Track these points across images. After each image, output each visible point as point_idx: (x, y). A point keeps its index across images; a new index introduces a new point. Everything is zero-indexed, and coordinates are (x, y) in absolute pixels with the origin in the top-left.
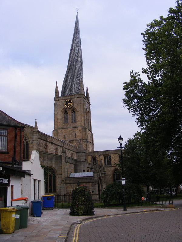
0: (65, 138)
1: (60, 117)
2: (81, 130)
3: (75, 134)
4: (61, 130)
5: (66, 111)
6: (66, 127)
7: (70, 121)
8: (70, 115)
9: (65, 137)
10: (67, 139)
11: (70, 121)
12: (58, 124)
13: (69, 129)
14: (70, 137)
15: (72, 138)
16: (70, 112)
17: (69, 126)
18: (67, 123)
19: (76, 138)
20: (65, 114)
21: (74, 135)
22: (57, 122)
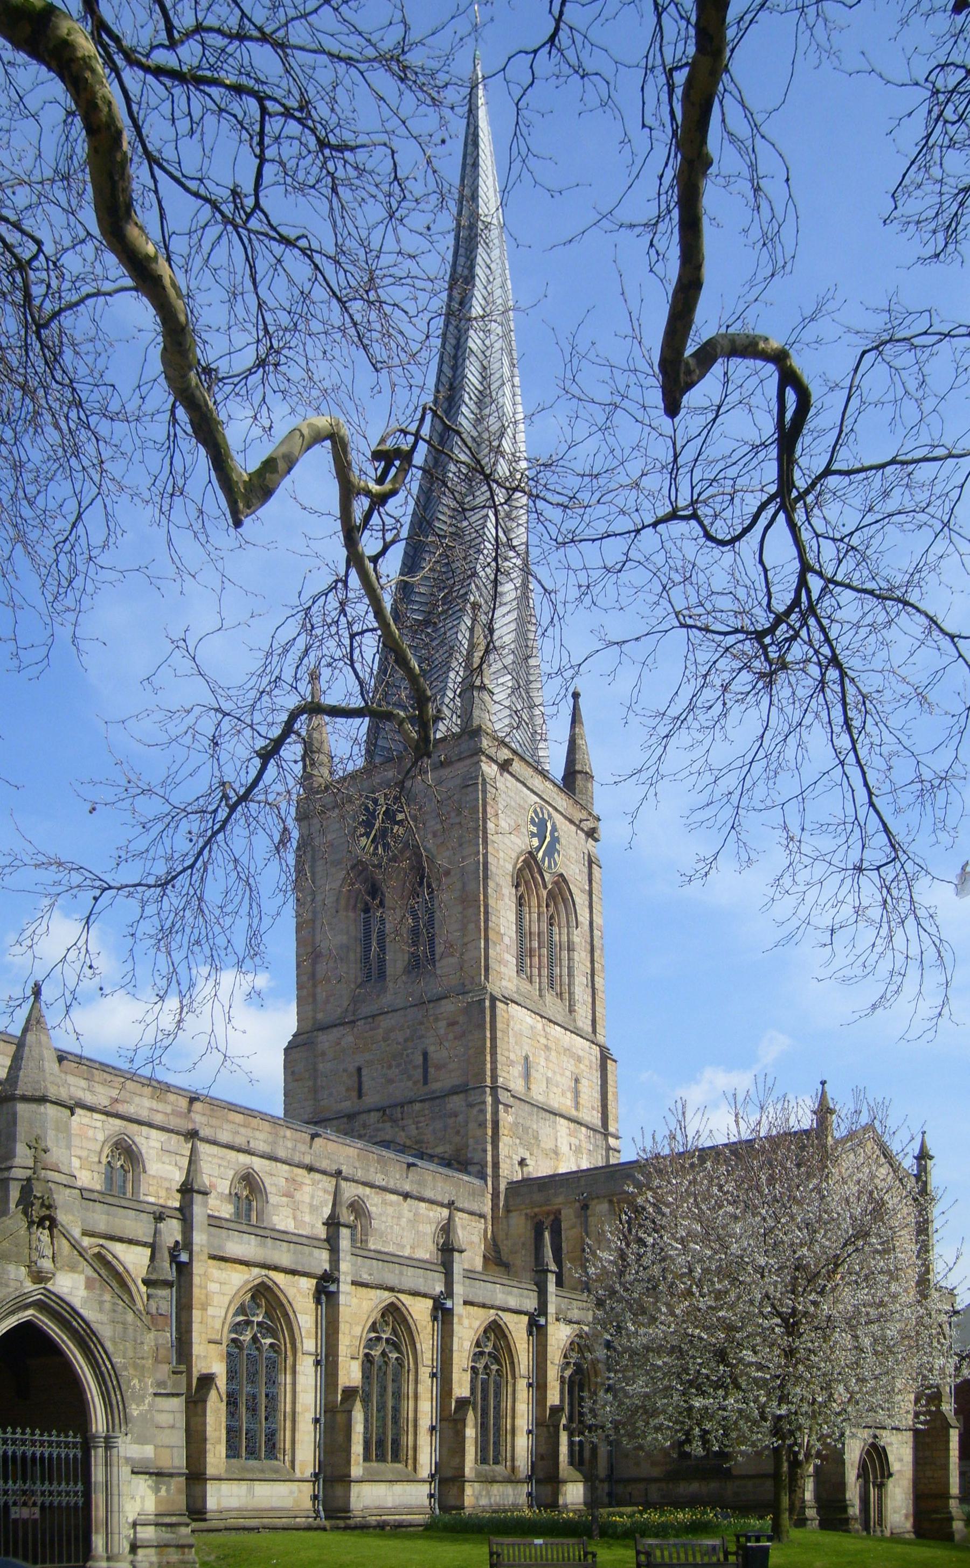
0: (360, 1096)
1: (338, 934)
2: (461, 1019)
3: (425, 1055)
4: (335, 1033)
5: (374, 890)
6: (365, 1010)
7: (397, 958)
8: (395, 918)
9: (360, 1083)
10: (371, 1099)
11: (397, 958)
12: (321, 994)
13: (385, 1023)
14: (391, 1081)
15: (403, 1089)
16: (392, 890)
17: (387, 1000)
18: (382, 975)
19: (426, 1082)
20: (367, 910)
21: (419, 1060)
22: (313, 975)
